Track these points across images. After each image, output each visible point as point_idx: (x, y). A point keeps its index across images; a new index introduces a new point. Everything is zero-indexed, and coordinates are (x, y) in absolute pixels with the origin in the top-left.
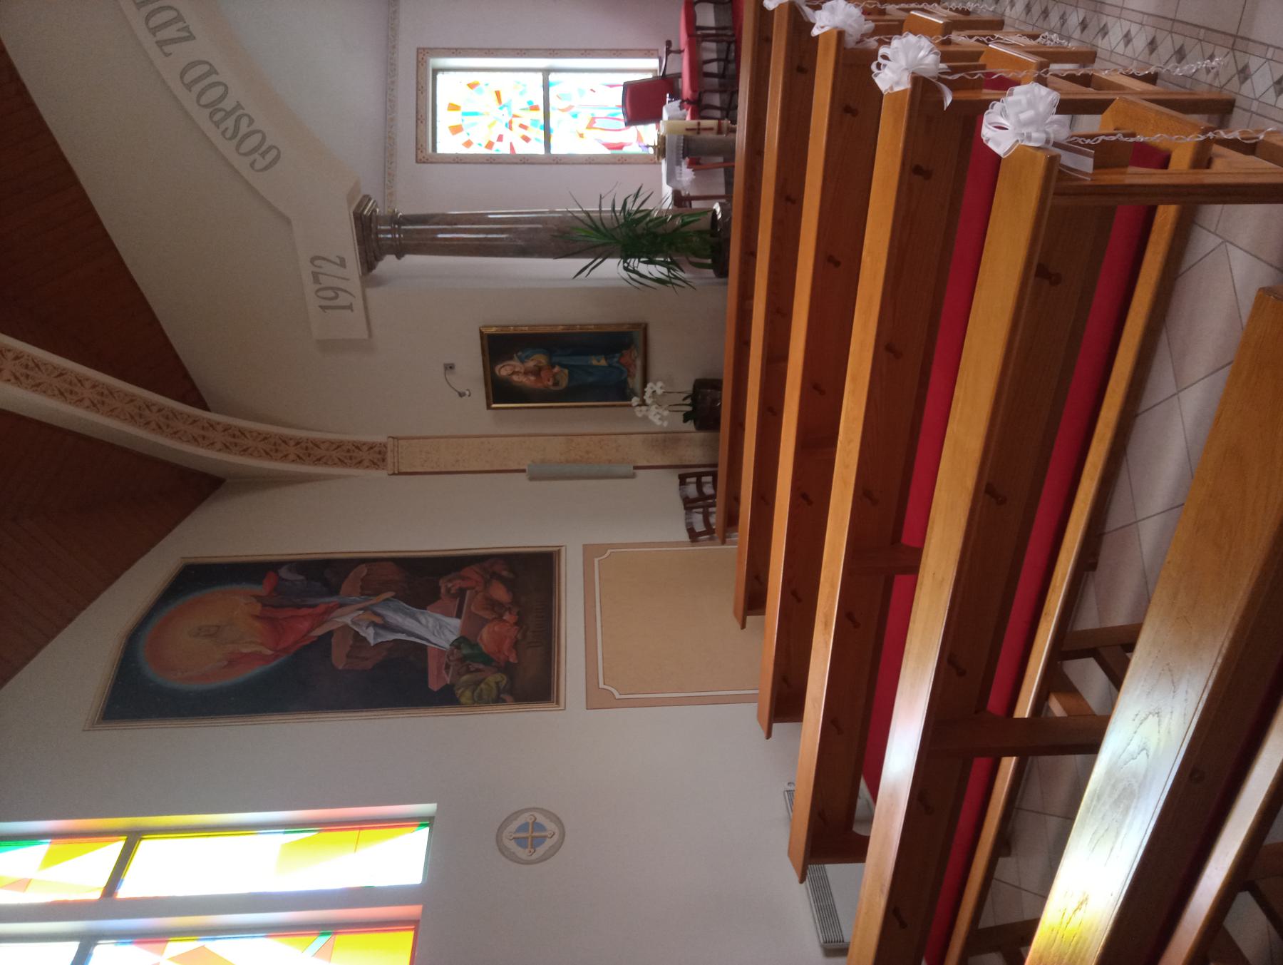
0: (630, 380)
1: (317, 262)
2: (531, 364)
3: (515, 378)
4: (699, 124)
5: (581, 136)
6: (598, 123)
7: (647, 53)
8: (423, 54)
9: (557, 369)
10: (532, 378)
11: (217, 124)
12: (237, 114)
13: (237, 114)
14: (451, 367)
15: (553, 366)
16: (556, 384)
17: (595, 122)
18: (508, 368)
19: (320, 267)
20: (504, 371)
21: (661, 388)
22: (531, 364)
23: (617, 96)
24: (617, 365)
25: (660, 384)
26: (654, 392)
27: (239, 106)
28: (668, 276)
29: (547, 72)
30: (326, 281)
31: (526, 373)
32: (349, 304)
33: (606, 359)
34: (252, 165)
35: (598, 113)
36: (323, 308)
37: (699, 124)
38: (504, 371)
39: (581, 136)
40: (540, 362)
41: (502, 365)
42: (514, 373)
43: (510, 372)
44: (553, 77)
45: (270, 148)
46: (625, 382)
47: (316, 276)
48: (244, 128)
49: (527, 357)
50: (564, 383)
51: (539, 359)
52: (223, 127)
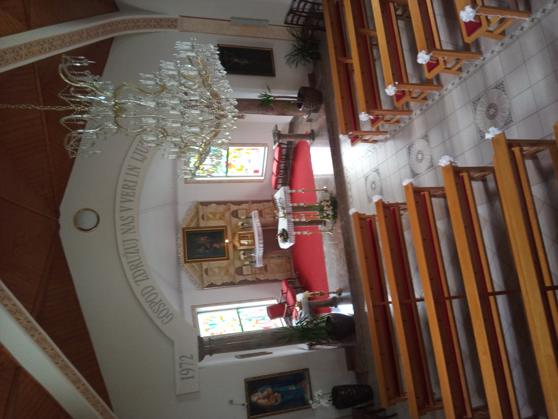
0: (305, 395)
1: (183, 358)
3: (260, 401)
5: (254, 326)
6: (259, 322)
7: (272, 298)
8: (193, 308)
9: (276, 394)
10: (266, 400)
11: (152, 308)
12: (160, 303)
13: (160, 303)
15: (274, 392)
16: (276, 402)
18: (256, 396)
19: (182, 360)
20: (254, 398)
21: (321, 392)
22: (265, 393)
23: (265, 312)
24: (299, 388)
27: (161, 301)
29: (237, 309)
30: (185, 367)
31: (264, 398)
34: (162, 321)
35: (259, 319)
36: (182, 379)
38: (254, 398)
39: (254, 326)
40: (269, 392)
41: (254, 396)
42: (259, 399)
43: (257, 398)
44: (239, 310)
45: (171, 314)
47: (181, 365)
48: (161, 309)
49: (264, 390)
50: (279, 401)
51: (268, 390)
52: (154, 308)
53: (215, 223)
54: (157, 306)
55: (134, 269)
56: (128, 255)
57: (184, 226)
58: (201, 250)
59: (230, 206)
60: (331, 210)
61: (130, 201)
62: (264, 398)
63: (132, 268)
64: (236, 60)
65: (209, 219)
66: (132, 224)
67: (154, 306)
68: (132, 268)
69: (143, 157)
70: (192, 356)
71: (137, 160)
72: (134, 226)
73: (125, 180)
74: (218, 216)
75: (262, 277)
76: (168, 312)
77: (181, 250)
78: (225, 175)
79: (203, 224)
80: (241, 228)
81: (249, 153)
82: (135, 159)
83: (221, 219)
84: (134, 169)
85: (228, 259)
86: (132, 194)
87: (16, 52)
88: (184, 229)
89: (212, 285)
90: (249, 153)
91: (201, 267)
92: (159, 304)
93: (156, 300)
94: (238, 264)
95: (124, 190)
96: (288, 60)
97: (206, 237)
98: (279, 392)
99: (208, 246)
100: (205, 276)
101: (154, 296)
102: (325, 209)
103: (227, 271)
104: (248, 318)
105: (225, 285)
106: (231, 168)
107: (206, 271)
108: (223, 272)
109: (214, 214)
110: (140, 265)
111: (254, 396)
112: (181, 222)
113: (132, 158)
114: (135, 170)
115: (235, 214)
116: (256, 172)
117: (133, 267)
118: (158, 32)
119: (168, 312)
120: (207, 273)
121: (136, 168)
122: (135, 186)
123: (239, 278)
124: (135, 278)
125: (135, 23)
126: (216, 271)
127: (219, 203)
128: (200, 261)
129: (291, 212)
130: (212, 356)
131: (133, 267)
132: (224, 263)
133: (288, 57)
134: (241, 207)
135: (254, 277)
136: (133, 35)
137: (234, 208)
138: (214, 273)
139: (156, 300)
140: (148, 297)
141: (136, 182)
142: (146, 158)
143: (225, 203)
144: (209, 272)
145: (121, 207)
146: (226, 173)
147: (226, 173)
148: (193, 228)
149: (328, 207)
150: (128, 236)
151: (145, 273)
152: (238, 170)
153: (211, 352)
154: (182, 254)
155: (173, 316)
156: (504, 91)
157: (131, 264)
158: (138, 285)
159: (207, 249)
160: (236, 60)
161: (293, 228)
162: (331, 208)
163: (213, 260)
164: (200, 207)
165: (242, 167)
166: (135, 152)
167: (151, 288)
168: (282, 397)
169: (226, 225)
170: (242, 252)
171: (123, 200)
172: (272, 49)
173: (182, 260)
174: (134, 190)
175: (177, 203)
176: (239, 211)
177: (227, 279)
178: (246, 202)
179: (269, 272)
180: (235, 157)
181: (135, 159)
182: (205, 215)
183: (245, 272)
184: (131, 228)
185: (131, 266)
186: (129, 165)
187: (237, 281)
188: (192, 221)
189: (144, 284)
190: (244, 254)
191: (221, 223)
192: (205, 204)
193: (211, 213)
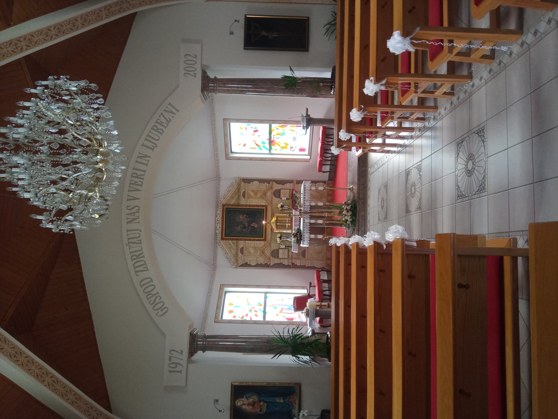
0: (293, 410)
1: (172, 352)
2: (251, 400)
3: (244, 407)
4: (321, 304)
5: (277, 315)
6: (284, 311)
7: (303, 288)
8: (222, 286)
9: (262, 403)
10: (251, 407)
11: (148, 299)
12: (156, 296)
13: (156, 296)
14: (217, 401)
15: (260, 401)
16: (261, 410)
17: (283, 311)
18: (241, 402)
20: (239, 403)
21: (307, 413)
22: (251, 400)
23: (291, 302)
24: (287, 402)
25: (306, 411)
26: (304, 415)
27: (158, 293)
28: (310, 360)
29: (266, 293)
30: (173, 360)
31: (249, 405)
32: (180, 370)
33: (283, 399)
34: (157, 314)
35: (284, 307)
36: (170, 372)
37: (321, 304)
38: (239, 403)
39: (277, 315)
40: (255, 400)
41: (239, 400)
43: (242, 404)
44: (268, 295)
45: (165, 308)
46: (291, 411)
47: (170, 357)
48: (157, 301)
49: (250, 397)
50: (264, 410)
51: (254, 398)
52: (150, 300)
53: (255, 202)
54: (154, 297)
55: (134, 259)
56: (130, 244)
57: (224, 202)
58: (239, 228)
59: (272, 184)
60: (350, 215)
61: (138, 190)
62: (249, 404)
63: (133, 258)
64: (264, 33)
65: (249, 197)
66: (137, 214)
67: (151, 297)
68: (133, 258)
69: (155, 145)
70: (182, 351)
71: (148, 147)
72: (139, 216)
73: (134, 169)
74: (259, 195)
75: (298, 263)
76: (163, 305)
77: (219, 226)
78: (268, 152)
79: (243, 202)
80: (281, 210)
81: (294, 131)
82: (146, 146)
83: (262, 197)
84: (143, 157)
85: (265, 240)
86: (140, 183)
87: (15, 44)
88: (223, 206)
89: (246, 265)
90: (294, 131)
91: (237, 246)
92: (155, 296)
93: (153, 292)
94: (274, 247)
95: (133, 179)
96: (328, 30)
97: (245, 215)
98: (264, 402)
99: (247, 225)
100: (240, 254)
101: (152, 287)
102: (344, 213)
103: (263, 252)
104: (274, 305)
105: (258, 266)
106: (274, 145)
107: (242, 250)
108: (259, 253)
109: (256, 193)
110: (142, 255)
111: (239, 401)
112: (222, 198)
113: (143, 145)
114: (146, 158)
115: (277, 194)
116: (302, 150)
117: (135, 257)
118: (182, 4)
119: (163, 305)
120: (242, 253)
121: (146, 156)
122: (144, 175)
123: (276, 261)
124: (135, 268)
125: (121, 8)
126: (252, 251)
127: (261, 181)
128: (237, 239)
129: (309, 212)
130: (205, 352)
131: (135, 257)
132: (260, 244)
133: (328, 26)
134: (284, 187)
135: (290, 261)
136: (161, 7)
137: (277, 187)
138: (249, 252)
139: (153, 292)
140: (145, 288)
141: (145, 171)
142: (157, 146)
143: (268, 181)
144: (245, 252)
145: (128, 196)
146: (270, 149)
147: (270, 149)
148: (232, 205)
149: (348, 211)
150: (133, 226)
151: (145, 264)
152: (283, 148)
153: (204, 349)
154: (220, 230)
155: (168, 310)
156: (483, 141)
157: (132, 254)
158: (137, 275)
159: (245, 227)
160: (264, 33)
161: (309, 227)
162: (350, 213)
163: (250, 240)
164: (243, 183)
165: (287, 144)
166: (146, 139)
167: (149, 280)
168: (267, 407)
169: (267, 204)
170: (279, 235)
171: (131, 189)
172: (308, 18)
173: (219, 236)
174: (143, 179)
175: (220, 178)
176: (282, 191)
177: (261, 260)
178: (291, 182)
179: (306, 258)
180: (278, 134)
181: (146, 146)
182: (246, 192)
183: (280, 256)
184: (135, 219)
185: (132, 256)
186: (140, 153)
187: (272, 264)
188: (232, 198)
189: (142, 275)
190: (280, 238)
191: (262, 202)
192: (248, 181)
193: (253, 191)
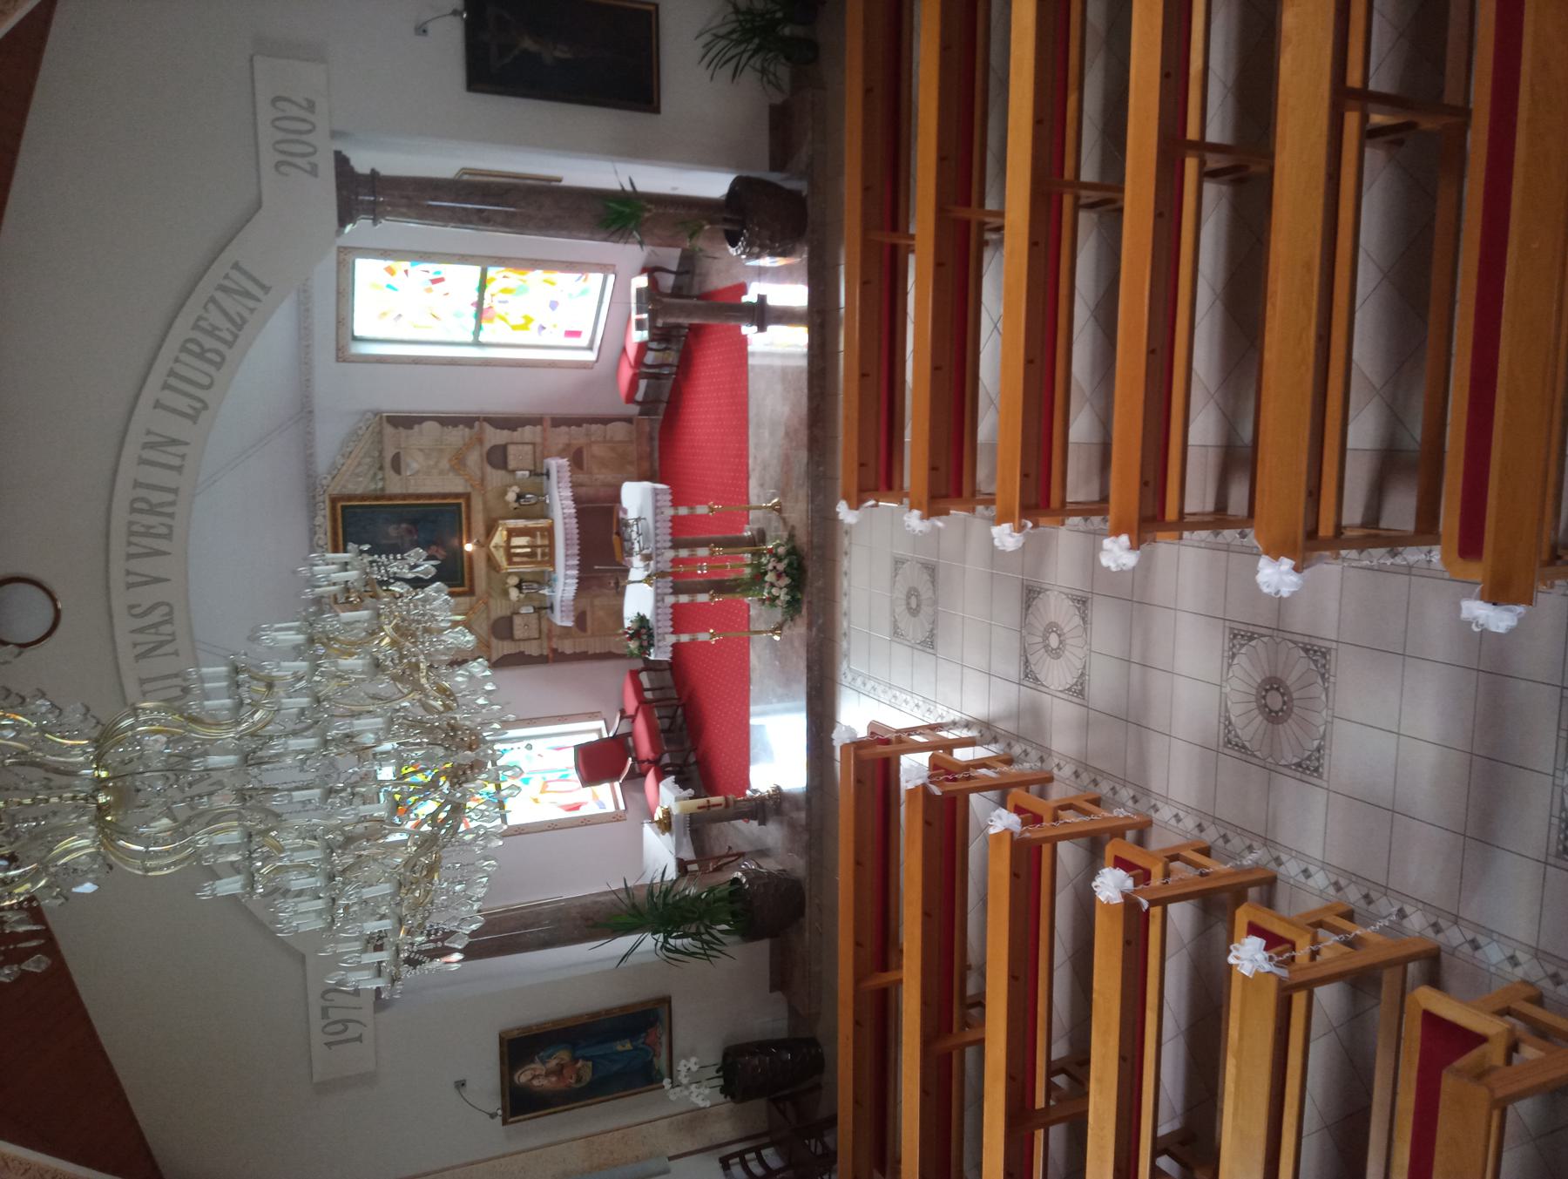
0: (655, 1060)
2: (553, 1063)
3: (536, 1083)
4: (708, 801)
6: (551, 786)
7: (592, 716)
9: (579, 1064)
10: (554, 1079)
14: (463, 1085)
15: (576, 1060)
16: (579, 1080)
17: (547, 786)
18: (528, 1073)
19: (332, 1000)
20: (523, 1077)
21: (696, 1064)
22: (553, 1063)
23: (568, 759)
24: (642, 1046)
25: (693, 1060)
26: (689, 1069)
28: (703, 948)
30: (335, 1015)
31: (548, 1074)
32: (357, 1035)
33: (631, 1042)
35: (549, 777)
36: (329, 1044)
37: (708, 801)
38: (523, 1077)
39: (536, 801)
40: (562, 1059)
42: (534, 1077)
43: (530, 1077)
46: (651, 1061)
47: (325, 1012)
49: (550, 1057)
50: (587, 1076)
51: (563, 1055)
59: (481, 429)
62: (548, 1074)
64: (528, 44)
66: (166, 629)
69: (198, 405)
71: (174, 411)
72: (173, 634)
75: (567, 647)
79: (395, 486)
81: (553, 284)
86: (163, 530)
94: (499, 609)
95: (137, 517)
96: (708, 47)
97: (404, 526)
98: (586, 1059)
102: (767, 578)
106: (491, 319)
112: (325, 478)
113: (158, 405)
115: (498, 457)
122: (173, 504)
134: (516, 435)
137: (495, 437)
141: (175, 491)
142: (206, 407)
143: (468, 421)
145: (128, 573)
147: (478, 328)
149: (779, 576)
152: (514, 328)
160: (528, 44)
162: (786, 581)
165: (528, 320)
166: (166, 386)
169: (469, 489)
170: (514, 581)
171: (133, 550)
172: (657, 6)
174: (171, 515)
175: (311, 412)
176: (512, 450)
178: (535, 421)
179: (589, 632)
180: (505, 291)
183: (518, 633)
186: (149, 433)
190: (519, 586)
191: (455, 485)
